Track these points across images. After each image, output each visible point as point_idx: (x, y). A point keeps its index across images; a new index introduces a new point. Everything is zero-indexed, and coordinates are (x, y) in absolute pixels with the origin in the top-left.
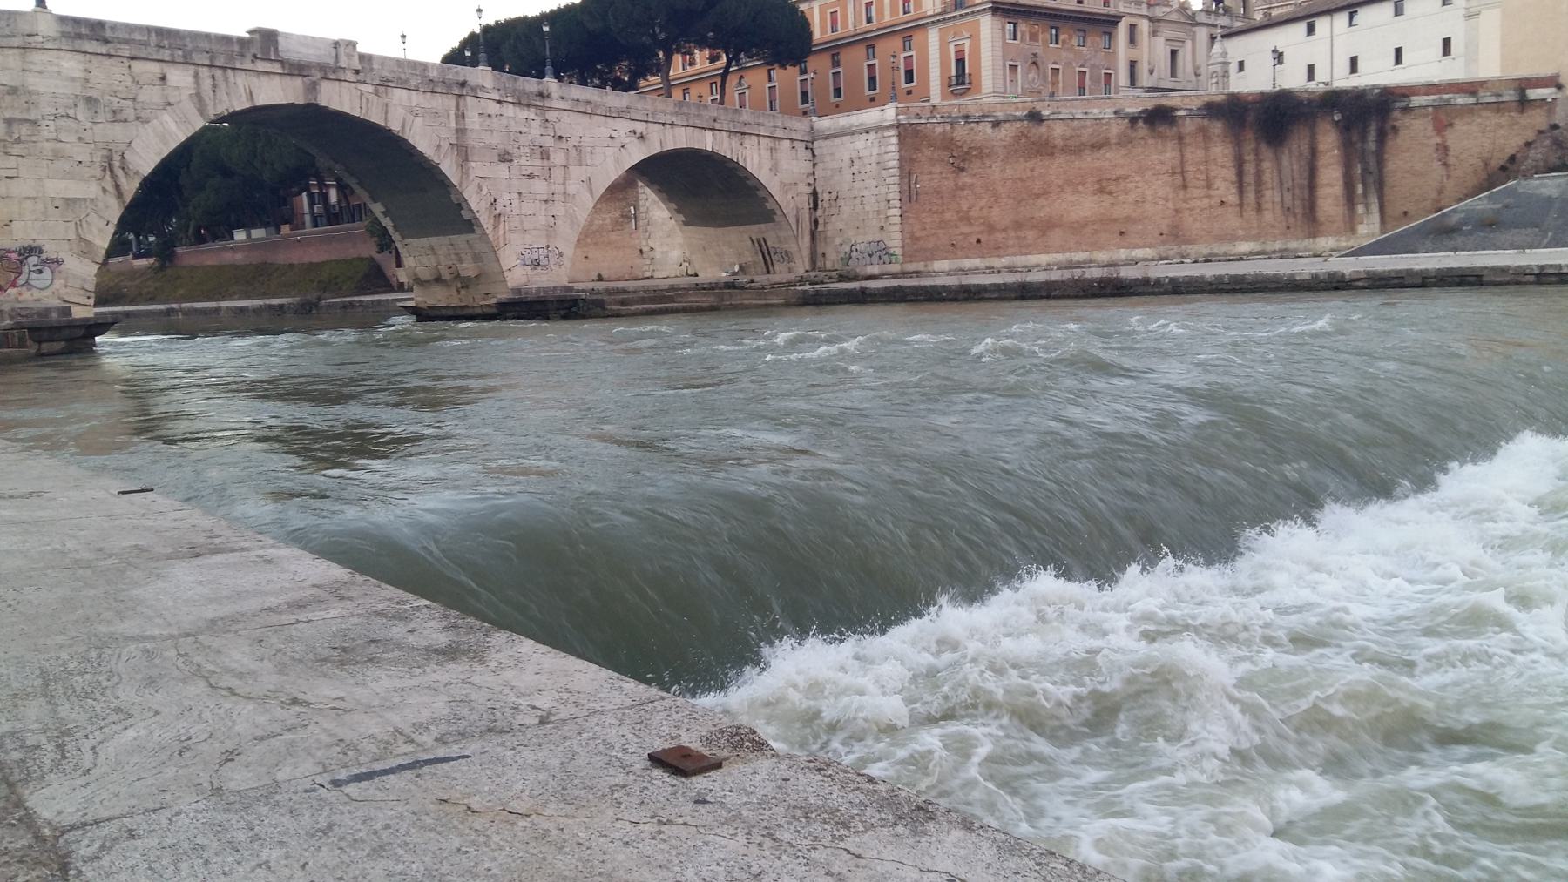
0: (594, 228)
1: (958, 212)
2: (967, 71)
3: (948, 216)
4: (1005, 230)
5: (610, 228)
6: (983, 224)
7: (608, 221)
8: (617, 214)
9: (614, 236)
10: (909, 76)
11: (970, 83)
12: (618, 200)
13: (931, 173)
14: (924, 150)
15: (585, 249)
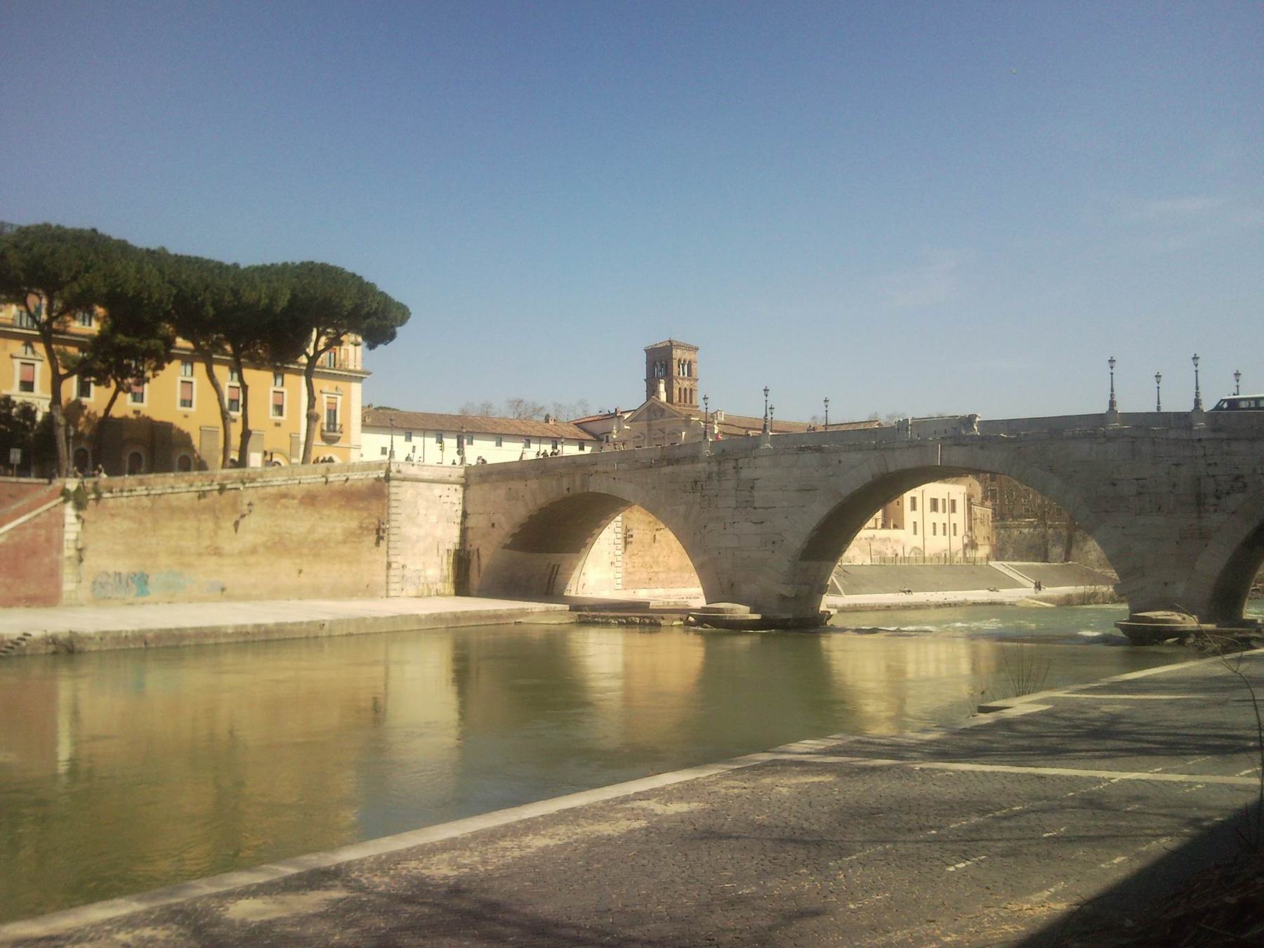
0: (316, 536)
1: (652, 557)
2: (338, 421)
3: (648, 559)
4: (675, 571)
5: (340, 538)
6: (665, 566)
7: (339, 531)
8: (354, 524)
9: (345, 549)
10: (279, 409)
11: (341, 432)
12: (358, 509)
13: (638, 529)
14: (635, 513)
15: (298, 561)
